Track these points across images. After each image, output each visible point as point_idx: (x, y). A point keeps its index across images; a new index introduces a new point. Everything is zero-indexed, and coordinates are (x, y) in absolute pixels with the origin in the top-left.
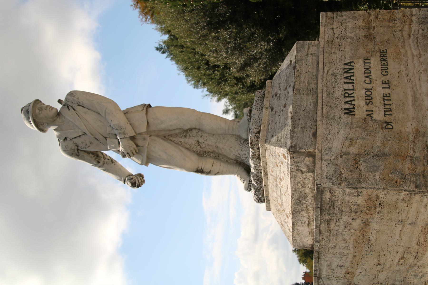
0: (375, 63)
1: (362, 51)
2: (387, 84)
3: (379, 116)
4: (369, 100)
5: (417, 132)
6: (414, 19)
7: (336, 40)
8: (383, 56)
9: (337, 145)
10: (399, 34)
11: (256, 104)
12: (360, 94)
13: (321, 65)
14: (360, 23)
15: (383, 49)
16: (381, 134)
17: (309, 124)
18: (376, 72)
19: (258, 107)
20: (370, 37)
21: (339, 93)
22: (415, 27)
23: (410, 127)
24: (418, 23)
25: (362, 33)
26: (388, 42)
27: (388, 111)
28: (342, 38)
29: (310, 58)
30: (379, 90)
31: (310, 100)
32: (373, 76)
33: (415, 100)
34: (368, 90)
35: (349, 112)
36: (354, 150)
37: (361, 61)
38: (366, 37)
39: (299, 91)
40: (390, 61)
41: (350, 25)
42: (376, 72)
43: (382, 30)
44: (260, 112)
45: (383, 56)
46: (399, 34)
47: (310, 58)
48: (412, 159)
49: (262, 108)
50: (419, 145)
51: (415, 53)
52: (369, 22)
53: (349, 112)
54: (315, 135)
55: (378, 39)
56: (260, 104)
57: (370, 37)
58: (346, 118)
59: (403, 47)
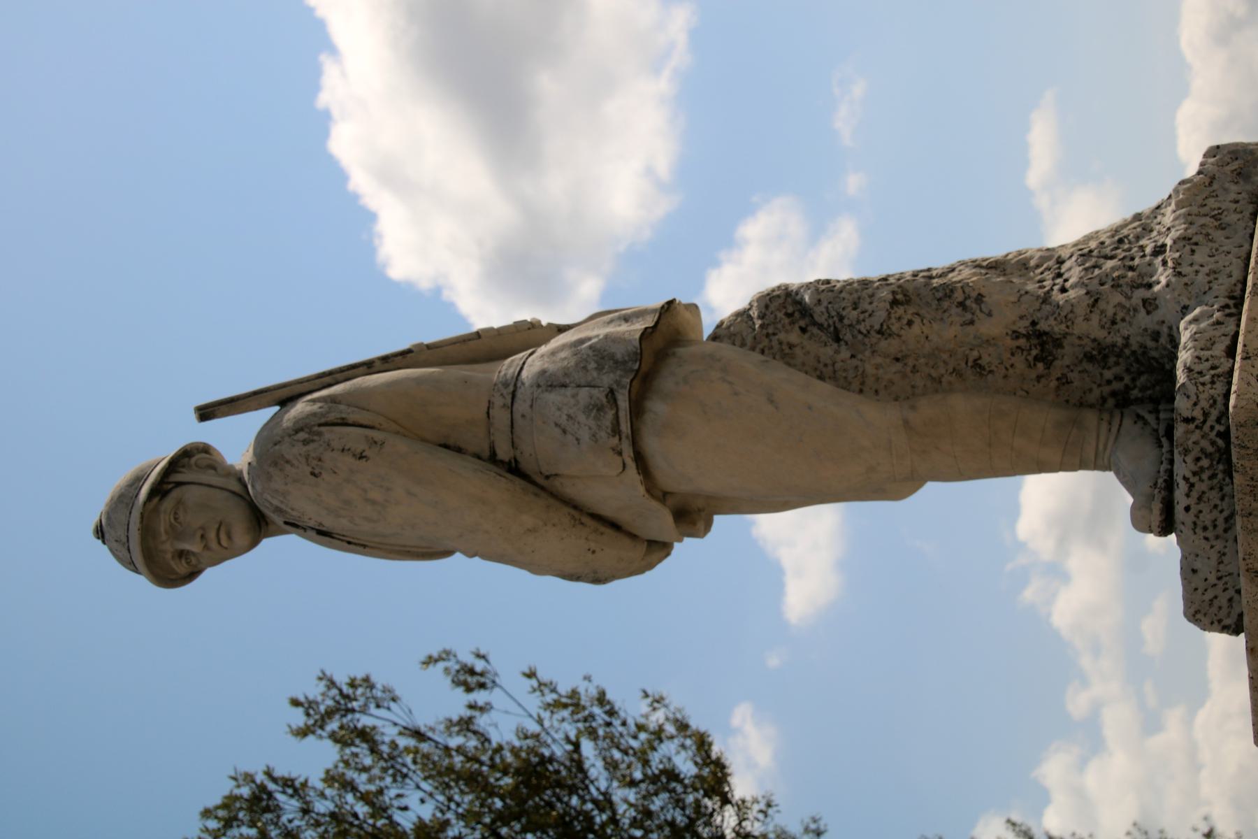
11: (1192, 501)
19: (1206, 518)
44: (1219, 545)
49: (1229, 519)
56: (1214, 496)
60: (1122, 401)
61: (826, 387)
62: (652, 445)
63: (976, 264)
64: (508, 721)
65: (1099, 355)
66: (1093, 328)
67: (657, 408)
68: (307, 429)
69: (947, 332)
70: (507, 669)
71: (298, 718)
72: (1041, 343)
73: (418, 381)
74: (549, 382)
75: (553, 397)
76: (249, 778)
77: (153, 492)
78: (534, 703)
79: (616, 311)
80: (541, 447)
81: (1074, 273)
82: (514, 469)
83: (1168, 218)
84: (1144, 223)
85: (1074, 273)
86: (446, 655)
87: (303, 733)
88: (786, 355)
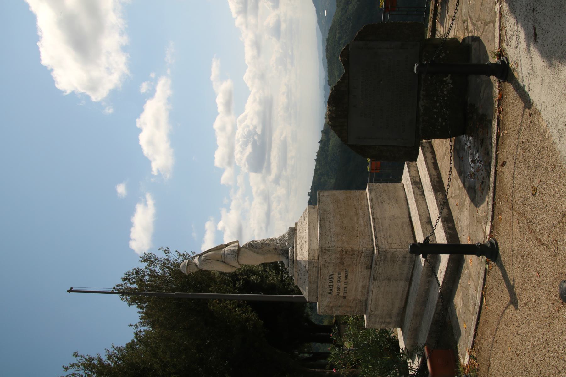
0: (343, 274)
1: (337, 269)
2: (346, 283)
3: (341, 294)
4: (338, 289)
5: (354, 299)
6: (363, 254)
7: (327, 264)
8: (347, 272)
9: (325, 304)
10: (355, 262)
12: (335, 286)
13: (319, 275)
14: (338, 256)
15: (347, 268)
16: (341, 300)
17: (315, 294)
18: (342, 279)
20: (342, 263)
21: (327, 286)
22: (362, 258)
23: (352, 298)
24: (364, 257)
25: (338, 261)
26: (349, 265)
27: (345, 292)
28: (329, 263)
29: (314, 269)
30: (343, 285)
31: (315, 285)
32: (341, 280)
33: (356, 289)
34: (338, 285)
35: (331, 293)
36: (331, 305)
37: (337, 274)
38: (340, 263)
39: (310, 282)
40: (349, 274)
41: (333, 256)
42: (342, 279)
43: (347, 260)
45: (347, 272)
46: (355, 262)
47: (314, 269)
48: (351, 307)
50: (354, 303)
51: (360, 270)
52: (342, 255)
53: (331, 293)
54: (317, 297)
55: (345, 264)
57: (342, 263)
58: (329, 295)
59: (356, 268)
60: (283, 254)
61: (255, 254)
62: (239, 260)
63: (269, 240)
64: (173, 257)
65: (281, 250)
66: (281, 248)
67: (240, 257)
68: (205, 260)
69: (267, 248)
70: (172, 251)
71: (141, 259)
72: (276, 249)
73: (214, 253)
74: (228, 254)
75: (229, 256)
76: (135, 269)
77: (188, 266)
78: (177, 256)
79: (231, 243)
80: (227, 260)
81: (278, 242)
82: (224, 262)
83: (286, 236)
84: (284, 236)
85: (278, 242)
86: (162, 248)
87: (142, 262)
88: (251, 250)
